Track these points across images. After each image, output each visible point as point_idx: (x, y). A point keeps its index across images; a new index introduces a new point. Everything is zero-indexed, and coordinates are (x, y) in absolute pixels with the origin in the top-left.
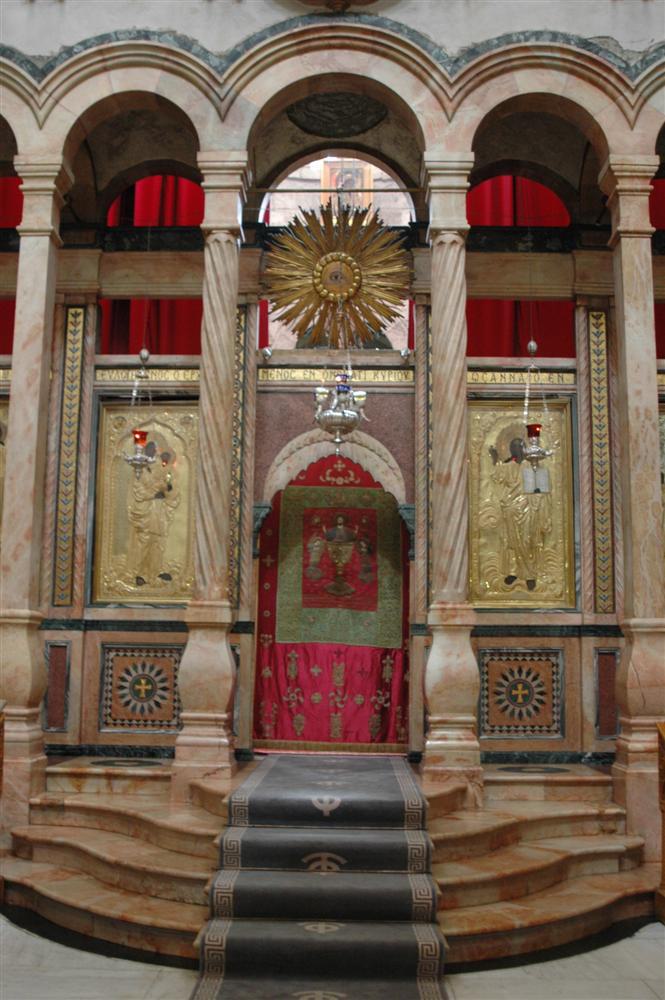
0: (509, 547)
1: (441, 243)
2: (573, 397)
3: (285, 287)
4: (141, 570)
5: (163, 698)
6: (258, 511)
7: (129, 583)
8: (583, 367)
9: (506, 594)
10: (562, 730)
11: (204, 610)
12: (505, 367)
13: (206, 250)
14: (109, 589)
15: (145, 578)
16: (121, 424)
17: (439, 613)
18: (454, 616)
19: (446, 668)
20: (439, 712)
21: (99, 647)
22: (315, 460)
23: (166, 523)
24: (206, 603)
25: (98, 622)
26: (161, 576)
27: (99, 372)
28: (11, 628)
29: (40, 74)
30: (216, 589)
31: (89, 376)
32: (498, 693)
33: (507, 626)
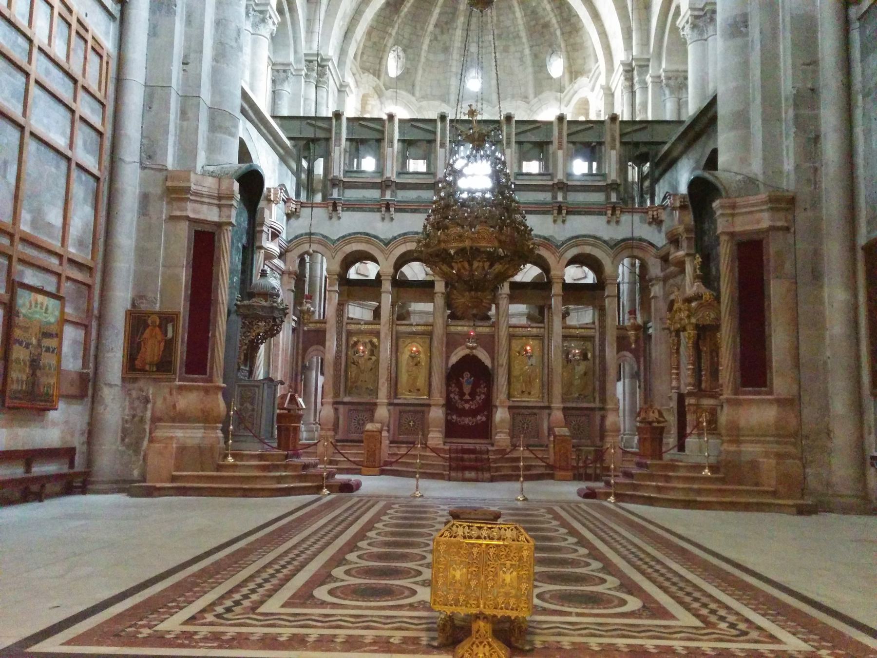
2: (543, 336)
8: (546, 327)
19: (501, 417)
29: (387, 244)
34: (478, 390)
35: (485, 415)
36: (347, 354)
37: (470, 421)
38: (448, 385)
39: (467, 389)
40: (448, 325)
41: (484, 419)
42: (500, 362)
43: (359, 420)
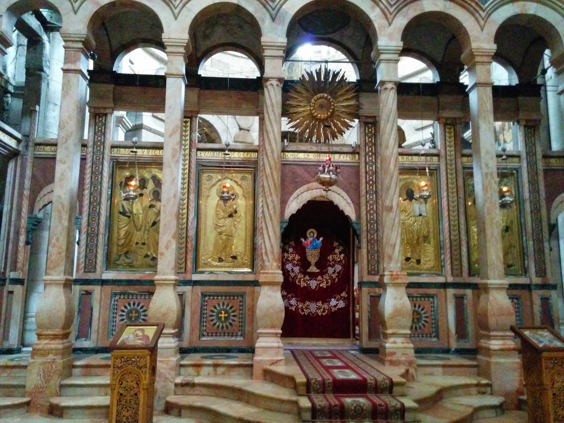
1: (386, 89)
3: (296, 111)
4: (221, 255)
5: (234, 321)
6: (282, 224)
7: (215, 261)
10: (437, 336)
11: (269, 275)
13: (265, 90)
14: (205, 264)
15: (223, 258)
16: (210, 179)
18: (397, 279)
19: (394, 306)
20: (392, 327)
21: (200, 294)
23: (234, 230)
24: (270, 271)
25: (199, 281)
26: (231, 257)
27: (199, 152)
28: (164, 286)
30: (275, 264)
31: (193, 154)
34: (330, 258)
35: (344, 299)
36: (111, 197)
37: (319, 308)
38: (284, 250)
39: (313, 256)
40: (284, 151)
41: (342, 304)
42: (387, 203)
43: (130, 311)
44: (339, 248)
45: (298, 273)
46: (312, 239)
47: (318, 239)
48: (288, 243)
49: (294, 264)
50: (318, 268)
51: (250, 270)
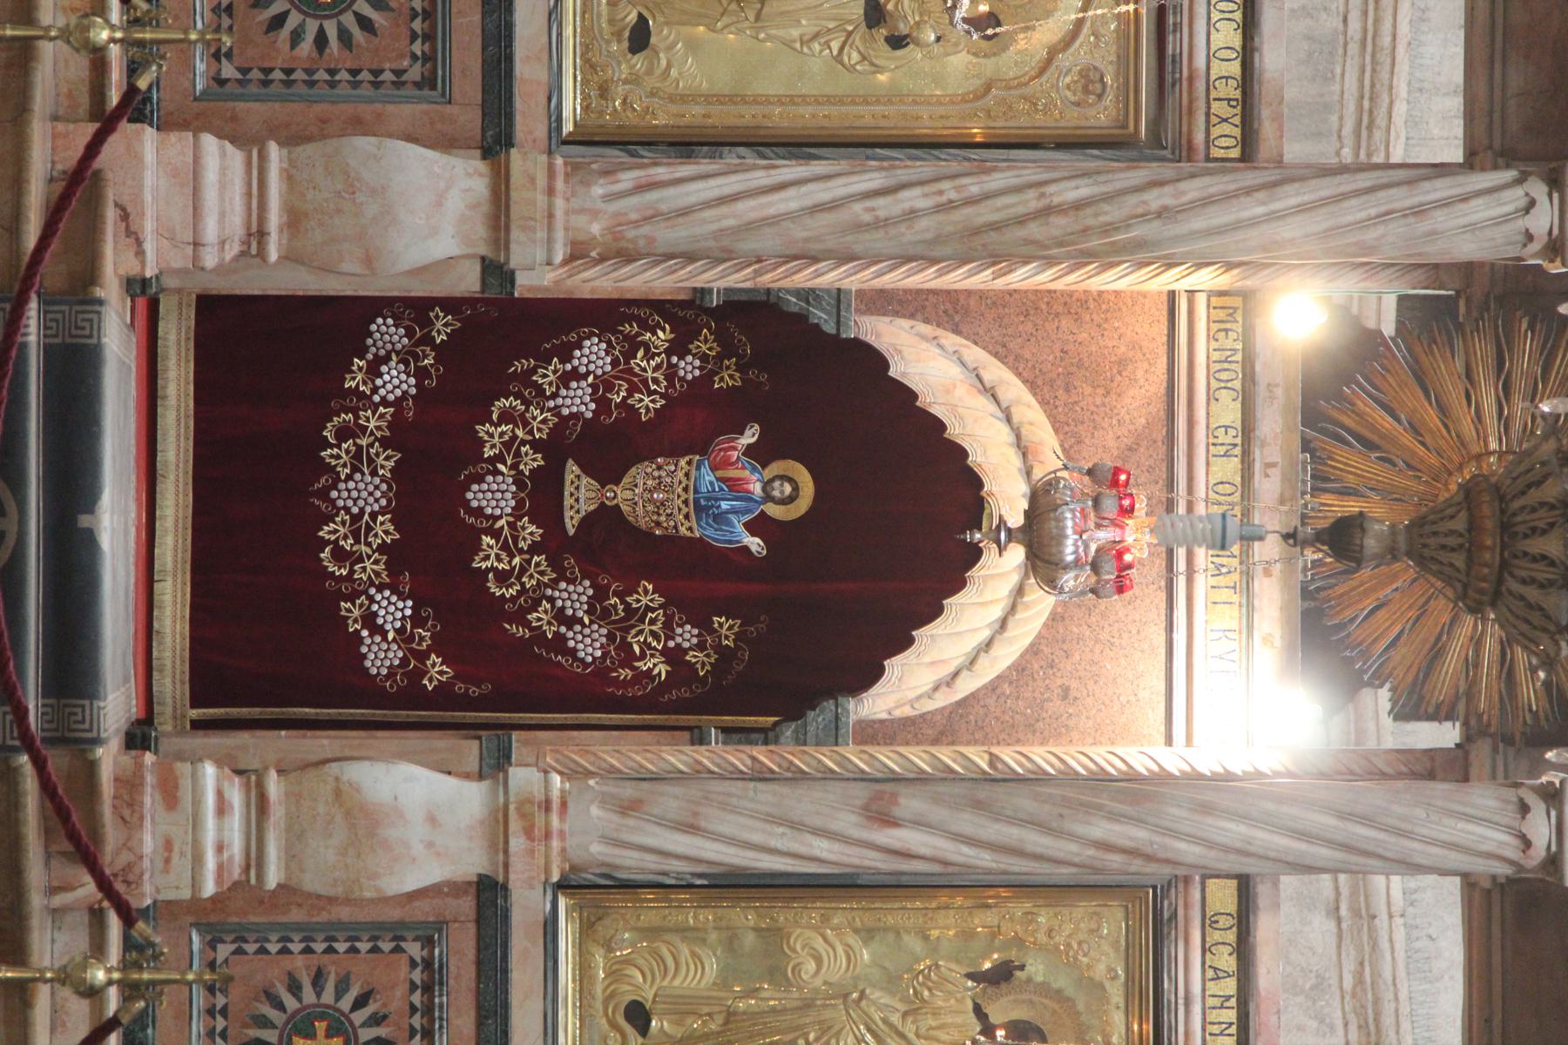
0: (730, 1015)
1: (1524, 809)
3: (1480, 374)
5: (296, 37)
9: (599, 1005)
11: (541, 199)
12: (1252, 1007)
13: (1509, 175)
17: (539, 796)
18: (529, 833)
20: (293, 797)
22: (976, 458)
24: (559, 203)
26: (642, 20)
30: (596, 229)
32: (318, 980)
33: (506, 1006)
34: (646, 596)
41: (380, 657)
44: (701, 646)
45: (556, 411)
46: (757, 489)
47: (751, 527)
48: (728, 348)
49: (609, 387)
50: (587, 522)
51: (568, 127)
